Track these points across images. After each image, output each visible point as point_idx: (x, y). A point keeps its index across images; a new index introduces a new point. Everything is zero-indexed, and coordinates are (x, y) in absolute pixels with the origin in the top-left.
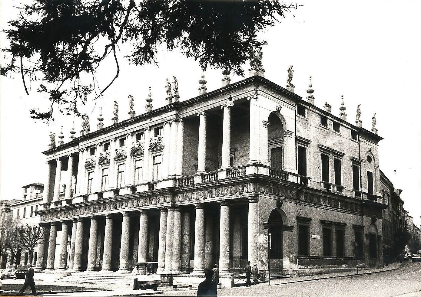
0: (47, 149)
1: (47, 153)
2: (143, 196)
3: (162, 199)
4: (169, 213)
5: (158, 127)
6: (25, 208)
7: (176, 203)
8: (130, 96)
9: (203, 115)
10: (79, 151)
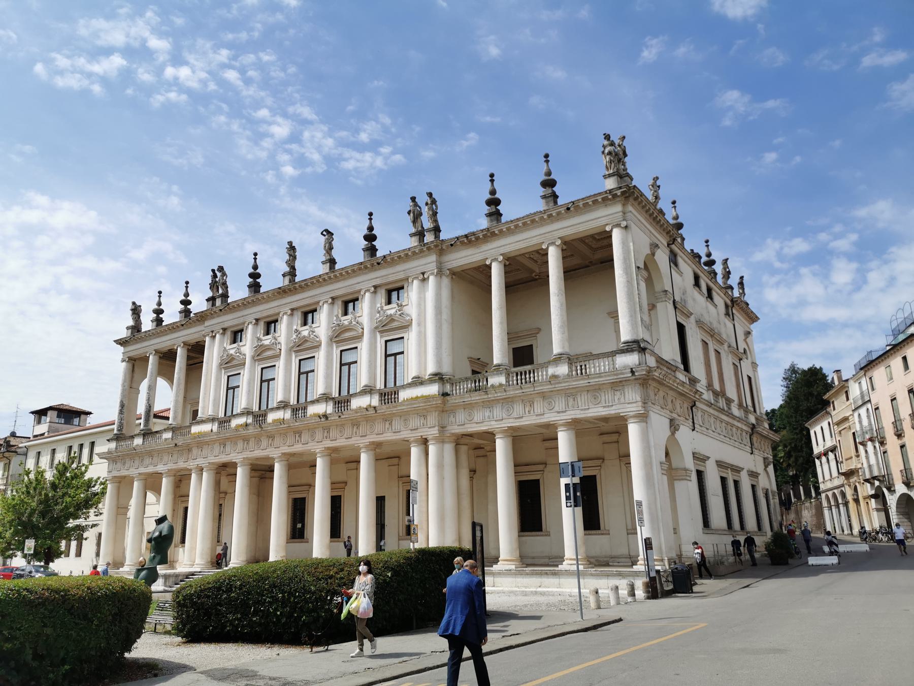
0: (124, 334)
1: (122, 342)
2: (369, 416)
3: (415, 422)
4: (432, 449)
5: (390, 287)
6: (905, 358)
7: (445, 427)
8: (327, 231)
9: (500, 262)
10: (205, 336)
